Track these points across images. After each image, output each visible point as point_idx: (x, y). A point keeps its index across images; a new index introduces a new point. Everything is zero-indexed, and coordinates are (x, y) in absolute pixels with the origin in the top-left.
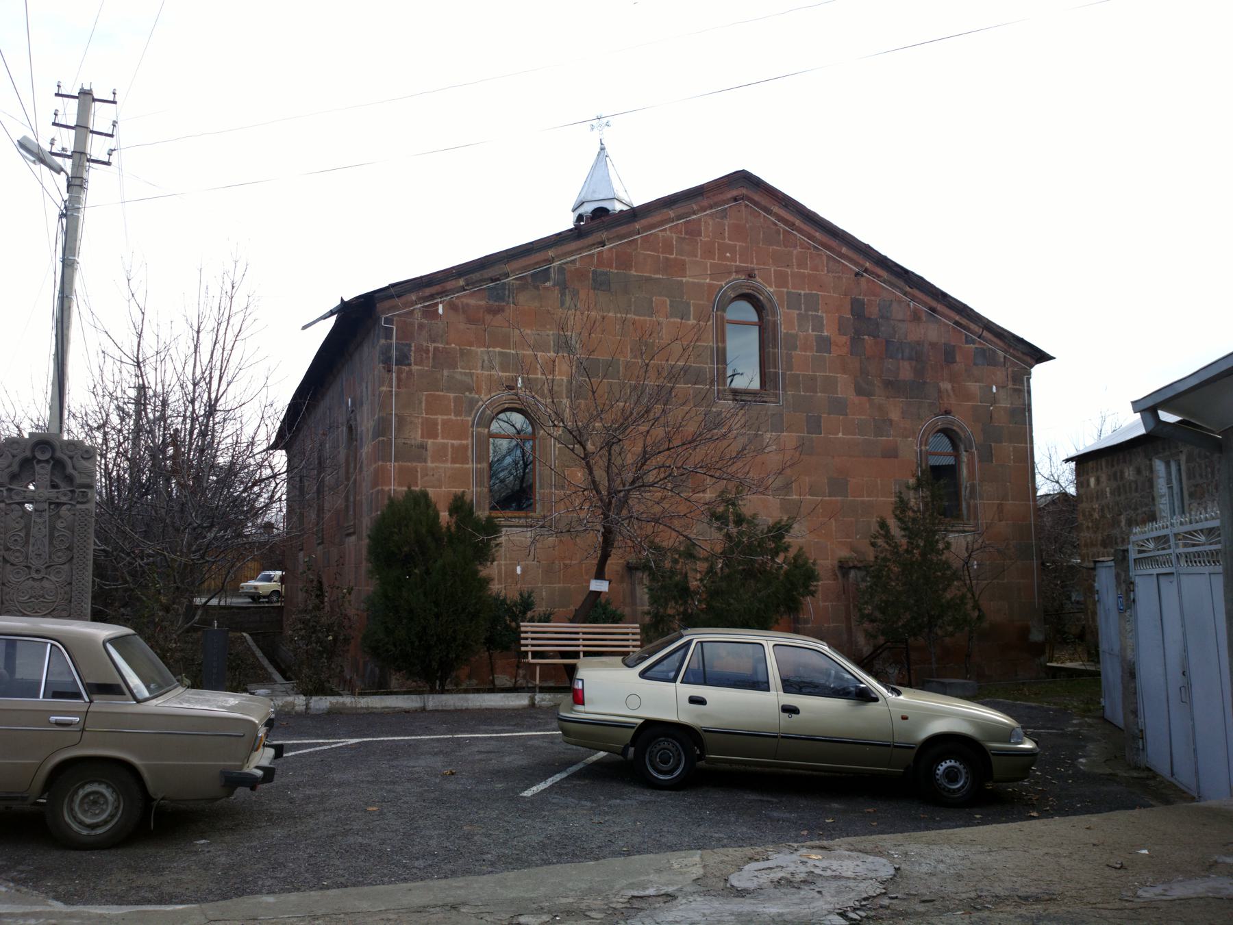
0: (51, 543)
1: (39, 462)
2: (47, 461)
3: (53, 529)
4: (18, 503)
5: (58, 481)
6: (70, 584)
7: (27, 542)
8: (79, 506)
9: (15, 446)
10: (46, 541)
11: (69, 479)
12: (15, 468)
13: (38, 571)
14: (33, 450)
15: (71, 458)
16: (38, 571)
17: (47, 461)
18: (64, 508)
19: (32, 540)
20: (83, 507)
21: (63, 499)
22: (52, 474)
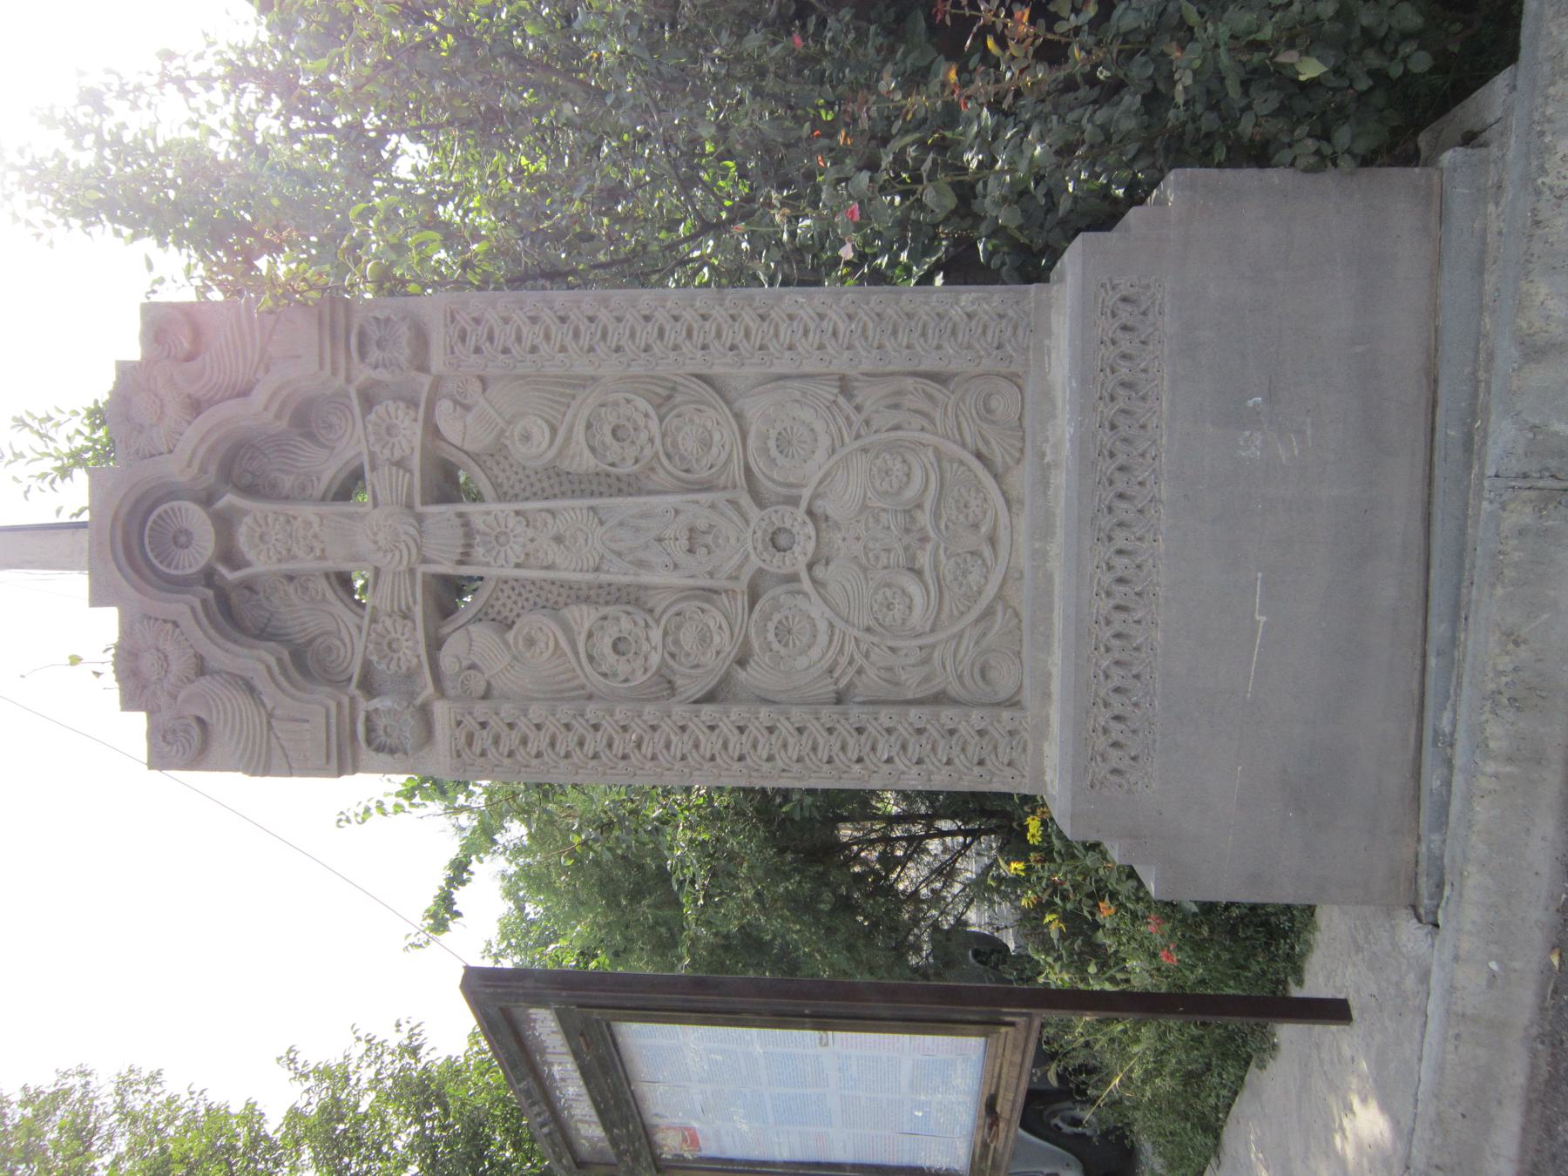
0: (629, 486)
1: (229, 556)
2: (225, 524)
3: (561, 482)
4: (435, 644)
5: (329, 470)
6: (845, 385)
7: (632, 598)
8: (437, 362)
9: (149, 663)
10: (627, 505)
11: (307, 419)
12: (256, 661)
13: (777, 541)
14: (179, 585)
15: (196, 407)
16: (777, 541)
17: (225, 524)
18: (450, 427)
19: (617, 575)
20: (438, 339)
21: (410, 434)
22: (299, 495)
